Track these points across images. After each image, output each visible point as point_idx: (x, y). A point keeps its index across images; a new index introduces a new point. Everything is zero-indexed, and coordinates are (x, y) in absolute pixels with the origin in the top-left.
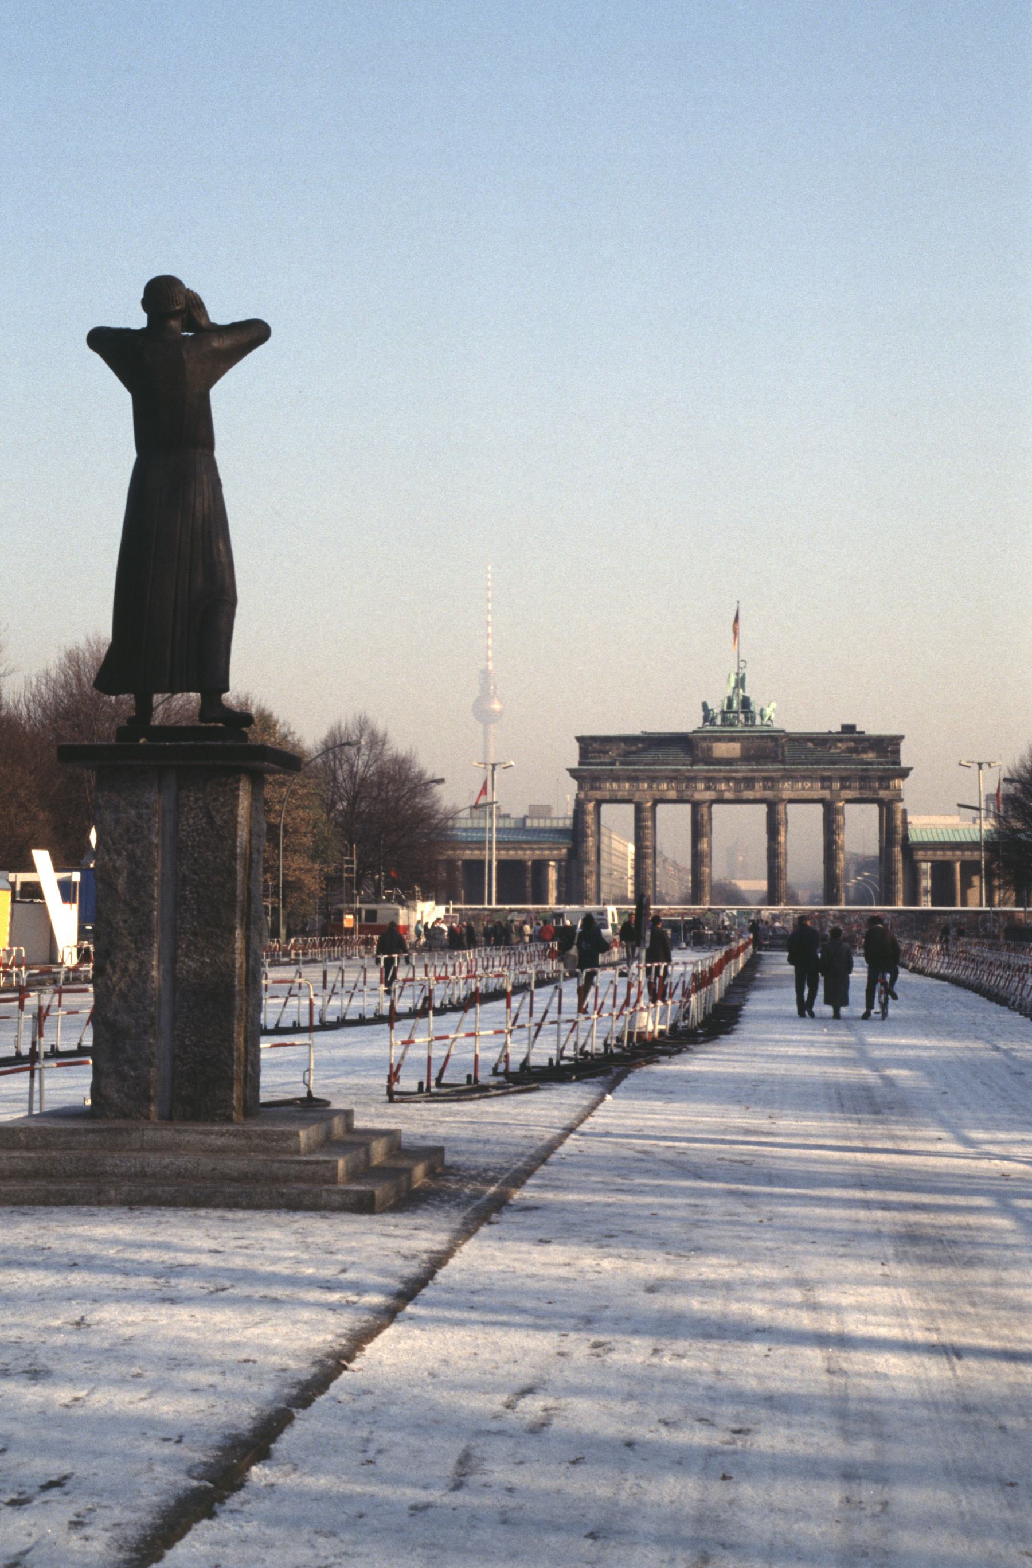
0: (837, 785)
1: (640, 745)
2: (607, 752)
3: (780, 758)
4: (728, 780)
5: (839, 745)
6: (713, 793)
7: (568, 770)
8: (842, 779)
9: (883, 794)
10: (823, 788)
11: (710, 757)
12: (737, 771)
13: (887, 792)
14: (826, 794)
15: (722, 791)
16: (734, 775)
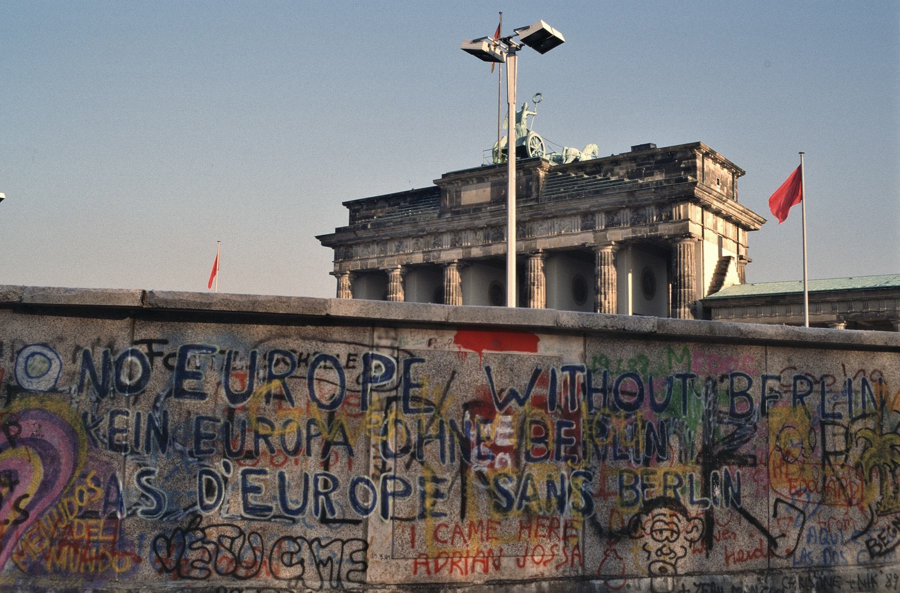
0: (601, 221)
1: (402, 204)
2: (372, 217)
3: (534, 195)
4: (475, 230)
5: (617, 169)
6: (461, 251)
7: (317, 237)
8: (611, 213)
9: (665, 230)
10: (585, 228)
11: (459, 205)
12: (479, 218)
13: (671, 226)
14: (588, 238)
15: (470, 247)
16: (477, 222)
